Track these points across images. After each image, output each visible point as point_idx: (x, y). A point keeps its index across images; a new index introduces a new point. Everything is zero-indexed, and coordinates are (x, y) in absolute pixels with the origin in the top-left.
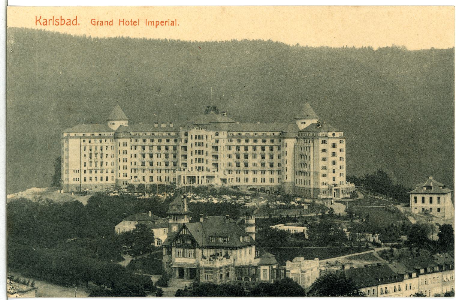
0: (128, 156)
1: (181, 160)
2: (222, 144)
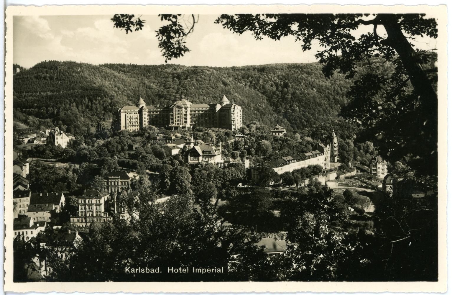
1: (171, 121)
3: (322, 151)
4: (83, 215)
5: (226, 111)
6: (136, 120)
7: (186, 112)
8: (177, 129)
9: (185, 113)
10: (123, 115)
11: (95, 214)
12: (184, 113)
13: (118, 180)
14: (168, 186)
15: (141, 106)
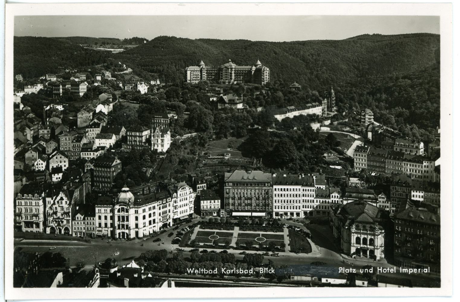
0: (205, 76)
1: (221, 77)
2: (233, 72)
3: (320, 104)
5: (259, 72)
6: (198, 76)
7: (232, 71)
10: (188, 73)
15: (202, 66)
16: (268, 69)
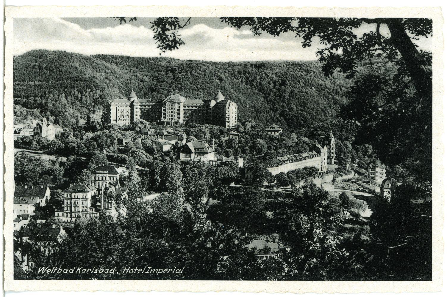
1: (163, 116)
2: (182, 108)
4: (69, 209)
5: (221, 107)
6: (127, 113)
7: (179, 107)
8: (170, 125)
9: (178, 108)
11: (80, 209)
12: (177, 108)
13: (106, 175)
14: (158, 182)
16: (235, 104)
